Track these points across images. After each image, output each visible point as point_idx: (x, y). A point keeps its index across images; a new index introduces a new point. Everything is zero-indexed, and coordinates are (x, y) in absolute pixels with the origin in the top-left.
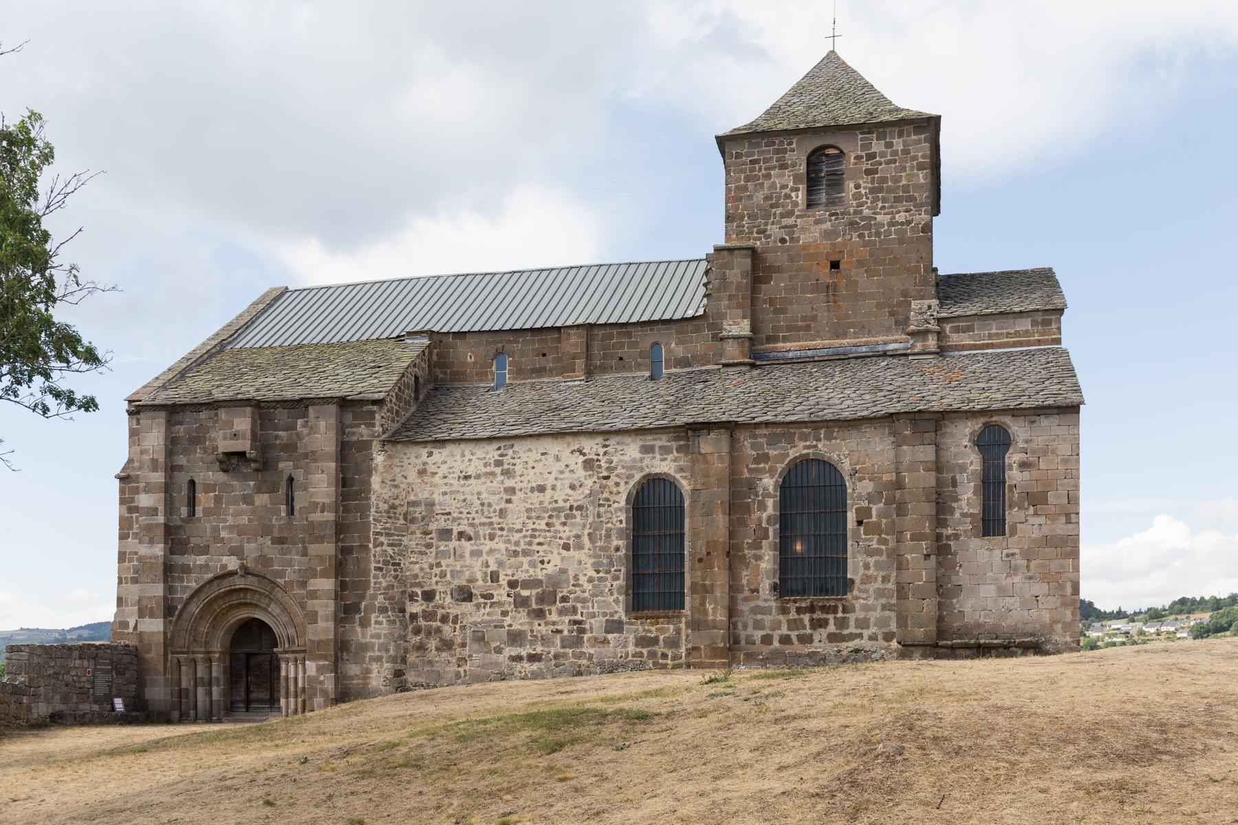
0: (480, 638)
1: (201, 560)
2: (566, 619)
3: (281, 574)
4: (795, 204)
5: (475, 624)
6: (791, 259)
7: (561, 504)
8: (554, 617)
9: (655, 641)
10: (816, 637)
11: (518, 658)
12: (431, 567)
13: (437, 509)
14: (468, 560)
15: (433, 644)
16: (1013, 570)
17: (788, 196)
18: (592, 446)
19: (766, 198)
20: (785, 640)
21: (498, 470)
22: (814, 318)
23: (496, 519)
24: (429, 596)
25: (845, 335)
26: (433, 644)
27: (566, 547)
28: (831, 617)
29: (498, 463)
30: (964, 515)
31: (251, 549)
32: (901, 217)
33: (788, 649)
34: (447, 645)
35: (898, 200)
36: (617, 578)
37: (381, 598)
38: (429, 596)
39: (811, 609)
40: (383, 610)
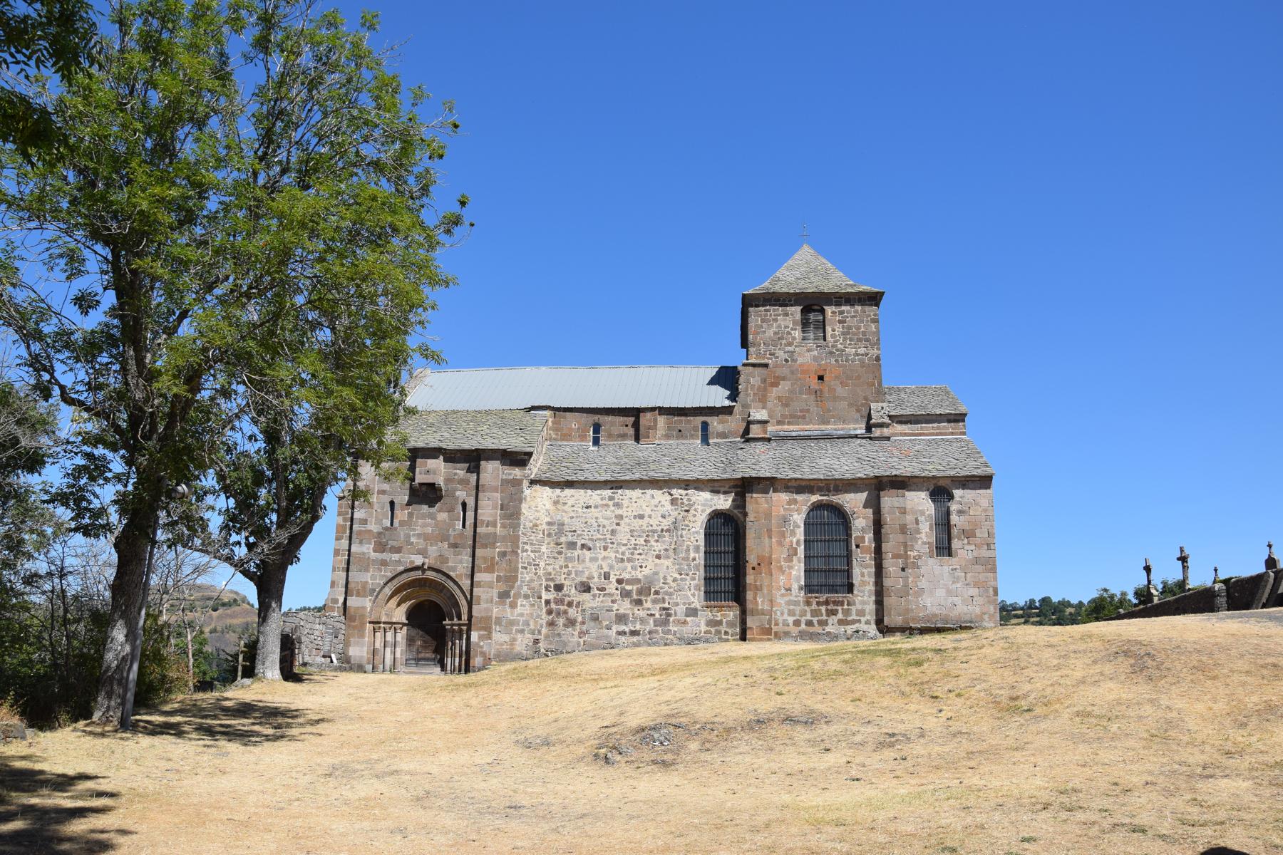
0: (596, 618)
1: (395, 557)
2: (658, 606)
3: (454, 569)
4: (794, 338)
5: (592, 608)
6: (792, 373)
7: (655, 527)
8: (648, 605)
9: (720, 623)
10: (830, 622)
11: (623, 633)
12: (561, 568)
13: (566, 528)
14: (588, 564)
15: (561, 621)
16: (956, 580)
17: (789, 333)
18: (677, 492)
19: (775, 333)
20: (809, 623)
21: (611, 503)
22: (808, 411)
23: (608, 536)
24: (559, 588)
25: (828, 423)
26: (561, 621)
27: (658, 557)
28: (839, 608)
29: (611, 498)
30: (924, 543)
31: (433, 551)
32: (862, 351)
33: (811, 630)
34: (571, 623)
35: (859, 340)
36: (694, 579)
37: (525, 588)
38: (559, 588)
39: (827, 603)
40: (526, 597)
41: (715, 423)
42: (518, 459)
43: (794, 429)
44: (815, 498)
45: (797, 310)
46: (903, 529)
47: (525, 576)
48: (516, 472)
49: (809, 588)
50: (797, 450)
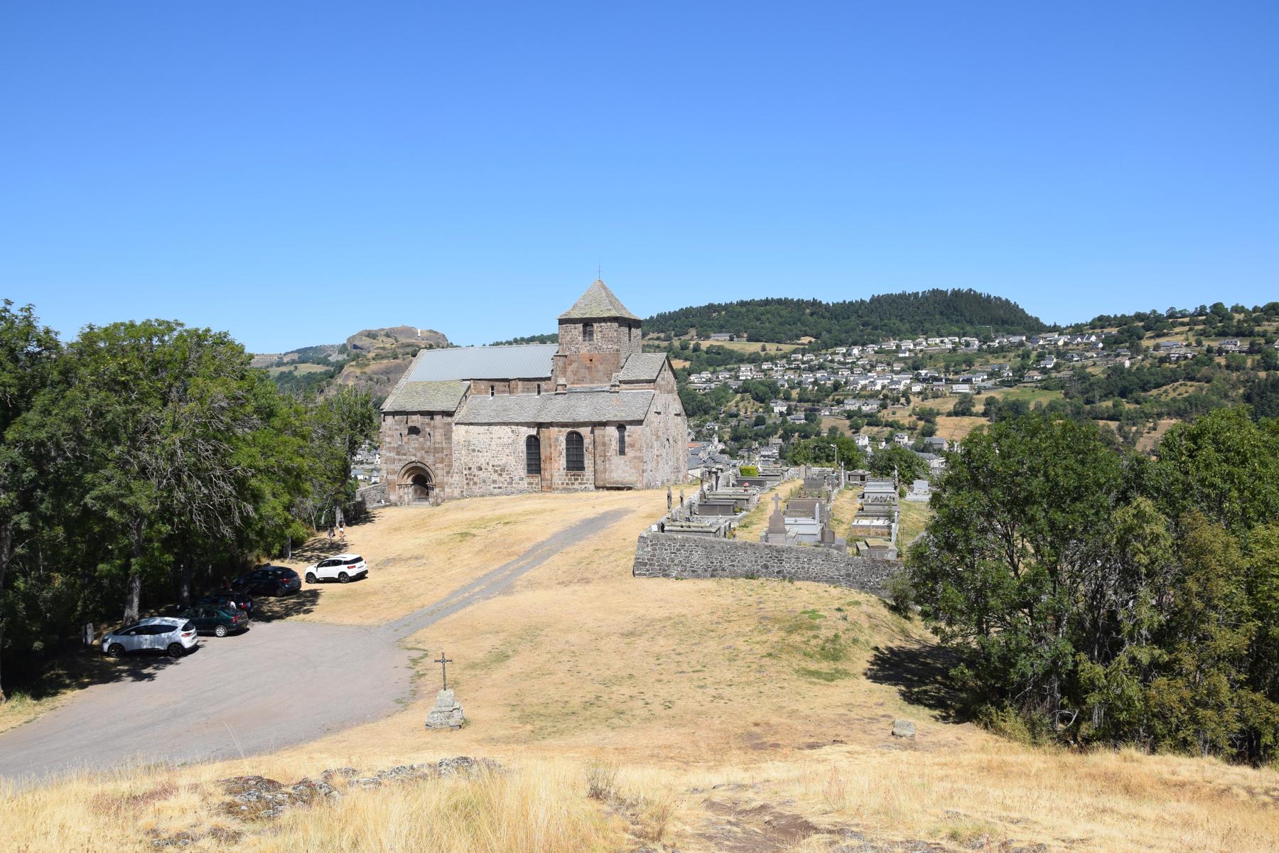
18: (514, 427)
34: (475, 483)
41: (543, 384)
42: (450, 414)
43: (578, 387)
44: (569, 430)
45: (580, 326)
46: (604, 444)
47: (456, 464)
48: (449, 419)
49: (568, 468)
50: (573, 400)
